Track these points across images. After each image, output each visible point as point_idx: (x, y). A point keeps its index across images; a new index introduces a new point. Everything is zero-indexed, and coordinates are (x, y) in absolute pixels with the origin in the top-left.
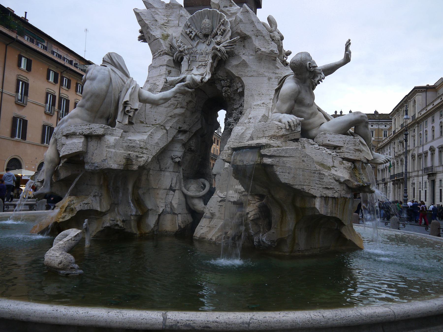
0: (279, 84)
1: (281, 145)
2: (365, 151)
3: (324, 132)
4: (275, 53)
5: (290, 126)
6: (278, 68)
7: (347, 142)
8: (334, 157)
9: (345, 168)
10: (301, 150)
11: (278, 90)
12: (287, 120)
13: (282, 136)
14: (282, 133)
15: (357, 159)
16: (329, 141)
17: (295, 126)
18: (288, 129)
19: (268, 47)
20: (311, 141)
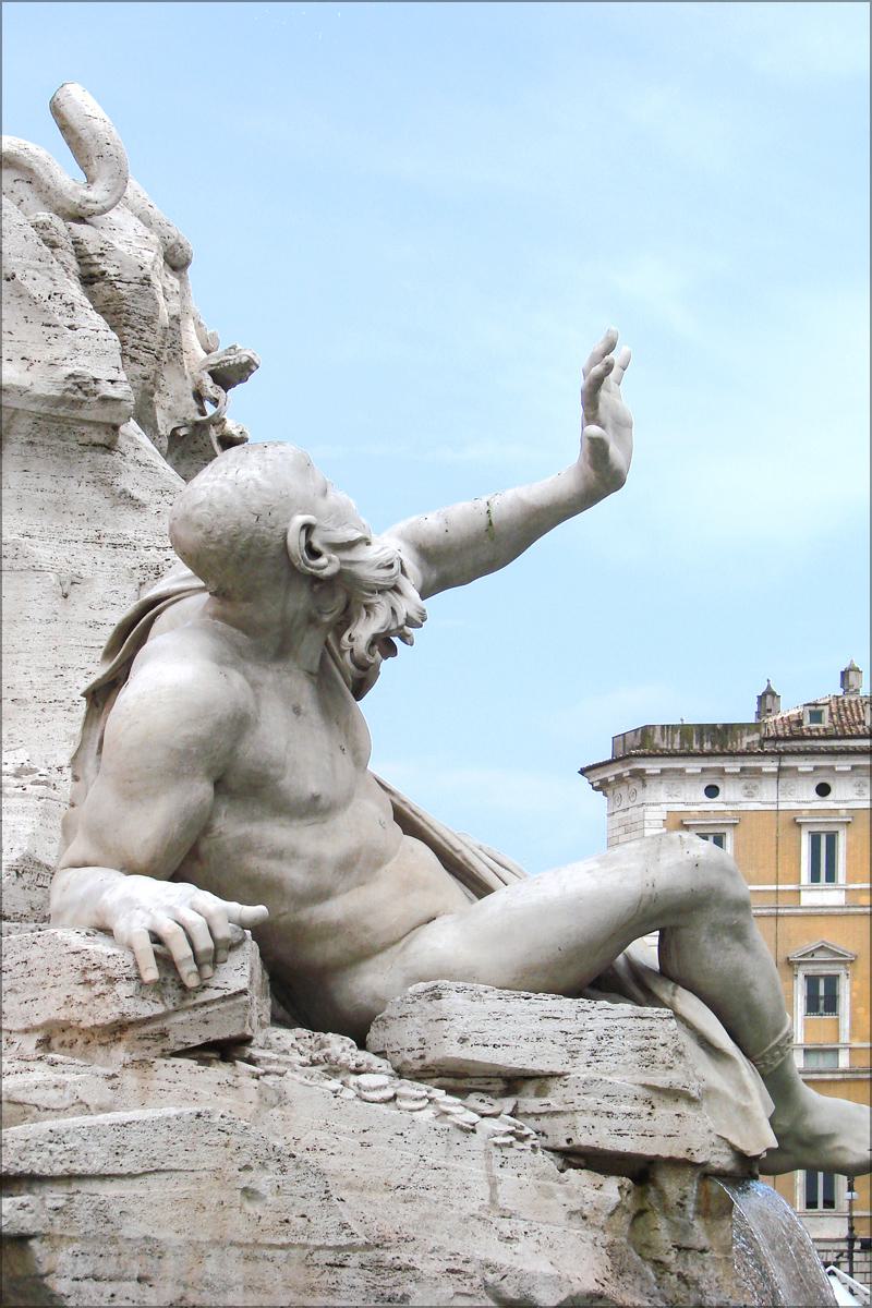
0: (110, 652)
1: (96, 1092)
2: (727, 1099)
3: (431, 984)
4: (105, 400)
5: (166, 961)
6: (137, 505)
7: (590, 1042)
8: (496, 1152)
9: (577, 1220)
10: (229, 1128)
11: (102, 695)
12: (147, 925)
13: (118, 1029)
14: (116, 1010)
15: (665, 1154)
16: (463, 1040)
17: (202, 959)
18: (158, 986)
19: (48, 355)
20: (339, 1046)
